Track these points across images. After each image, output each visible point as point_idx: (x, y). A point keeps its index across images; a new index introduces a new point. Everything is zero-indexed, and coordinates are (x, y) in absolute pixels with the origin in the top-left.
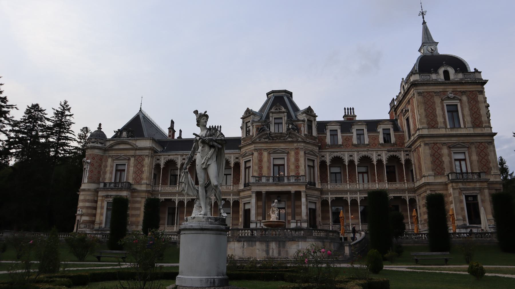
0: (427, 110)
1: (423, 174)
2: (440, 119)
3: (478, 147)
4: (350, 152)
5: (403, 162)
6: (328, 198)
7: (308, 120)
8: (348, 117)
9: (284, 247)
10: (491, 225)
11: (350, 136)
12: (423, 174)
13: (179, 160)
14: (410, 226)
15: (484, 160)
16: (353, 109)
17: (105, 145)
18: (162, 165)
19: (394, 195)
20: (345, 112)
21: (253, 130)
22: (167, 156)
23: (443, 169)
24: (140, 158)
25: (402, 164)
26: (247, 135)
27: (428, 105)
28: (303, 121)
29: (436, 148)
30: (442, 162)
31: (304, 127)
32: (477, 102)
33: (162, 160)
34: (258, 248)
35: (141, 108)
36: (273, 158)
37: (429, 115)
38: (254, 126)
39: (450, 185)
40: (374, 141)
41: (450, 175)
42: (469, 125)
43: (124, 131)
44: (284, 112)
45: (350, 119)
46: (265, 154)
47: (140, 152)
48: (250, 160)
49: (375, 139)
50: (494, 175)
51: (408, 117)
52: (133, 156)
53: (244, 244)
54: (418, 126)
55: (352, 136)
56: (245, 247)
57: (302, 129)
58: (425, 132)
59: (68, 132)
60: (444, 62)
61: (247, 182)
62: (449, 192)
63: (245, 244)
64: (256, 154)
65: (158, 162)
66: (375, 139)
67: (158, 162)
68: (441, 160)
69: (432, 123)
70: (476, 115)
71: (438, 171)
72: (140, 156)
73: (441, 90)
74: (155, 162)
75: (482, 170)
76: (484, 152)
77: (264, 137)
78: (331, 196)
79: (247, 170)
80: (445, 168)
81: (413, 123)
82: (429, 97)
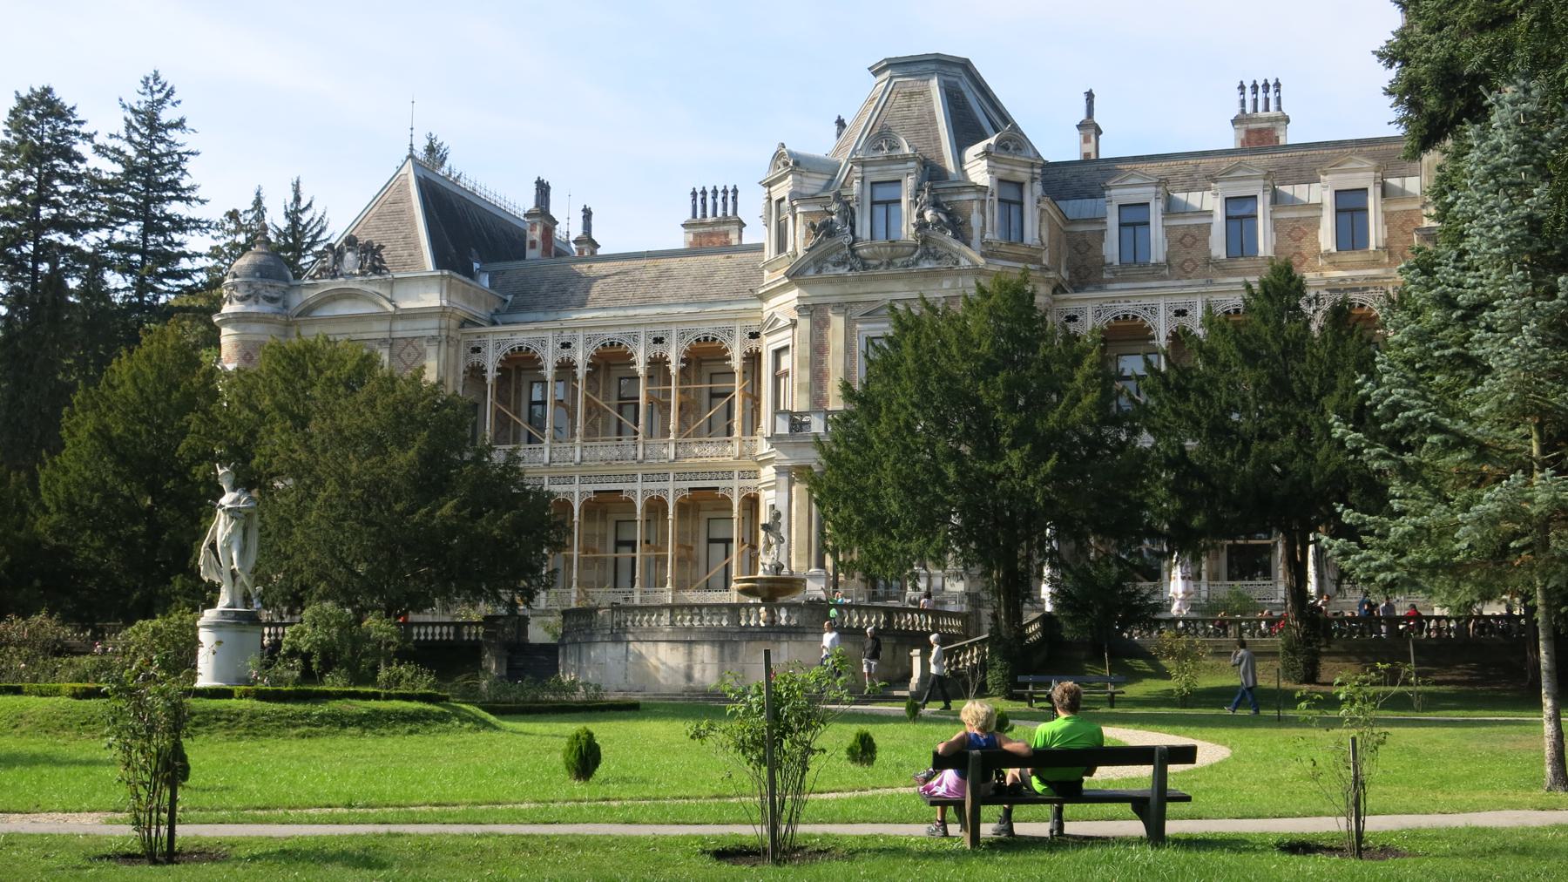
4: (1176, 300)
7: (1001, 181)
8: (1253, 126)
11: (1198, 226)
13: (550, 348)
16: (1277, 85)
17: (286, 307)
18: (490, 371)
20: (1243, 102)
22: (507, 336)
24: (410, 349)
31: (983, 213)
33: (490, 351)
35: (412, 149)
40: (1297, 244)
43: (349, 250)
45: (1260, 131)
46: (837, 323)
47: (409, 325)
52: (385, 340)
55: (1209, 225)
57: (975, 219)
59: (179, 198)
64: (805, 324)
65: (476, 358)
67: (476, 358)
72: (409, 341)
74: (466, 358)
77: (833, 258)
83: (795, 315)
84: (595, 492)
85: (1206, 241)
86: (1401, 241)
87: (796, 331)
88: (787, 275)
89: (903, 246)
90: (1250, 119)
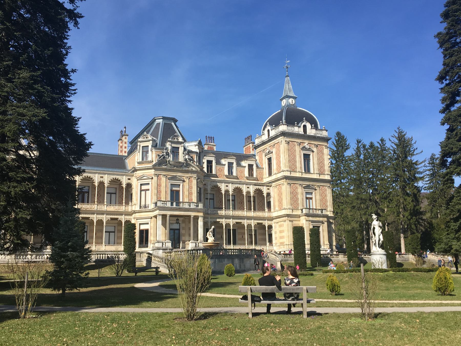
1: (284, 207)
2: (298, 165)
5: (265, 195)
6: (208, 221)
9: (243, 263)
12: (284, 207)
14: (268, 247)
15: (324, 200)
23: (298, 204)
26: (143, 159)
28: (196, 153)
30: (297, 199)
32: (323, 154)
38: (154, 152)
39: (304, 217)
41: (304, 210)
44: (181, 143)
45: (211, 147)
48: (149, 183)
53: (215, 261)
54: (283, 168)
56: (216, 262)
58: (288, 174)
60: (304, 118)
61: (143, 203)
62: (302, 223)
63: (216, 260)
64: (155, 178)
73: (301, 141)
79: (143, 193)
81: (277, 164)
84: (110, 218)
87: (153, 180)
88: (153, 166)
90: (209, 145)
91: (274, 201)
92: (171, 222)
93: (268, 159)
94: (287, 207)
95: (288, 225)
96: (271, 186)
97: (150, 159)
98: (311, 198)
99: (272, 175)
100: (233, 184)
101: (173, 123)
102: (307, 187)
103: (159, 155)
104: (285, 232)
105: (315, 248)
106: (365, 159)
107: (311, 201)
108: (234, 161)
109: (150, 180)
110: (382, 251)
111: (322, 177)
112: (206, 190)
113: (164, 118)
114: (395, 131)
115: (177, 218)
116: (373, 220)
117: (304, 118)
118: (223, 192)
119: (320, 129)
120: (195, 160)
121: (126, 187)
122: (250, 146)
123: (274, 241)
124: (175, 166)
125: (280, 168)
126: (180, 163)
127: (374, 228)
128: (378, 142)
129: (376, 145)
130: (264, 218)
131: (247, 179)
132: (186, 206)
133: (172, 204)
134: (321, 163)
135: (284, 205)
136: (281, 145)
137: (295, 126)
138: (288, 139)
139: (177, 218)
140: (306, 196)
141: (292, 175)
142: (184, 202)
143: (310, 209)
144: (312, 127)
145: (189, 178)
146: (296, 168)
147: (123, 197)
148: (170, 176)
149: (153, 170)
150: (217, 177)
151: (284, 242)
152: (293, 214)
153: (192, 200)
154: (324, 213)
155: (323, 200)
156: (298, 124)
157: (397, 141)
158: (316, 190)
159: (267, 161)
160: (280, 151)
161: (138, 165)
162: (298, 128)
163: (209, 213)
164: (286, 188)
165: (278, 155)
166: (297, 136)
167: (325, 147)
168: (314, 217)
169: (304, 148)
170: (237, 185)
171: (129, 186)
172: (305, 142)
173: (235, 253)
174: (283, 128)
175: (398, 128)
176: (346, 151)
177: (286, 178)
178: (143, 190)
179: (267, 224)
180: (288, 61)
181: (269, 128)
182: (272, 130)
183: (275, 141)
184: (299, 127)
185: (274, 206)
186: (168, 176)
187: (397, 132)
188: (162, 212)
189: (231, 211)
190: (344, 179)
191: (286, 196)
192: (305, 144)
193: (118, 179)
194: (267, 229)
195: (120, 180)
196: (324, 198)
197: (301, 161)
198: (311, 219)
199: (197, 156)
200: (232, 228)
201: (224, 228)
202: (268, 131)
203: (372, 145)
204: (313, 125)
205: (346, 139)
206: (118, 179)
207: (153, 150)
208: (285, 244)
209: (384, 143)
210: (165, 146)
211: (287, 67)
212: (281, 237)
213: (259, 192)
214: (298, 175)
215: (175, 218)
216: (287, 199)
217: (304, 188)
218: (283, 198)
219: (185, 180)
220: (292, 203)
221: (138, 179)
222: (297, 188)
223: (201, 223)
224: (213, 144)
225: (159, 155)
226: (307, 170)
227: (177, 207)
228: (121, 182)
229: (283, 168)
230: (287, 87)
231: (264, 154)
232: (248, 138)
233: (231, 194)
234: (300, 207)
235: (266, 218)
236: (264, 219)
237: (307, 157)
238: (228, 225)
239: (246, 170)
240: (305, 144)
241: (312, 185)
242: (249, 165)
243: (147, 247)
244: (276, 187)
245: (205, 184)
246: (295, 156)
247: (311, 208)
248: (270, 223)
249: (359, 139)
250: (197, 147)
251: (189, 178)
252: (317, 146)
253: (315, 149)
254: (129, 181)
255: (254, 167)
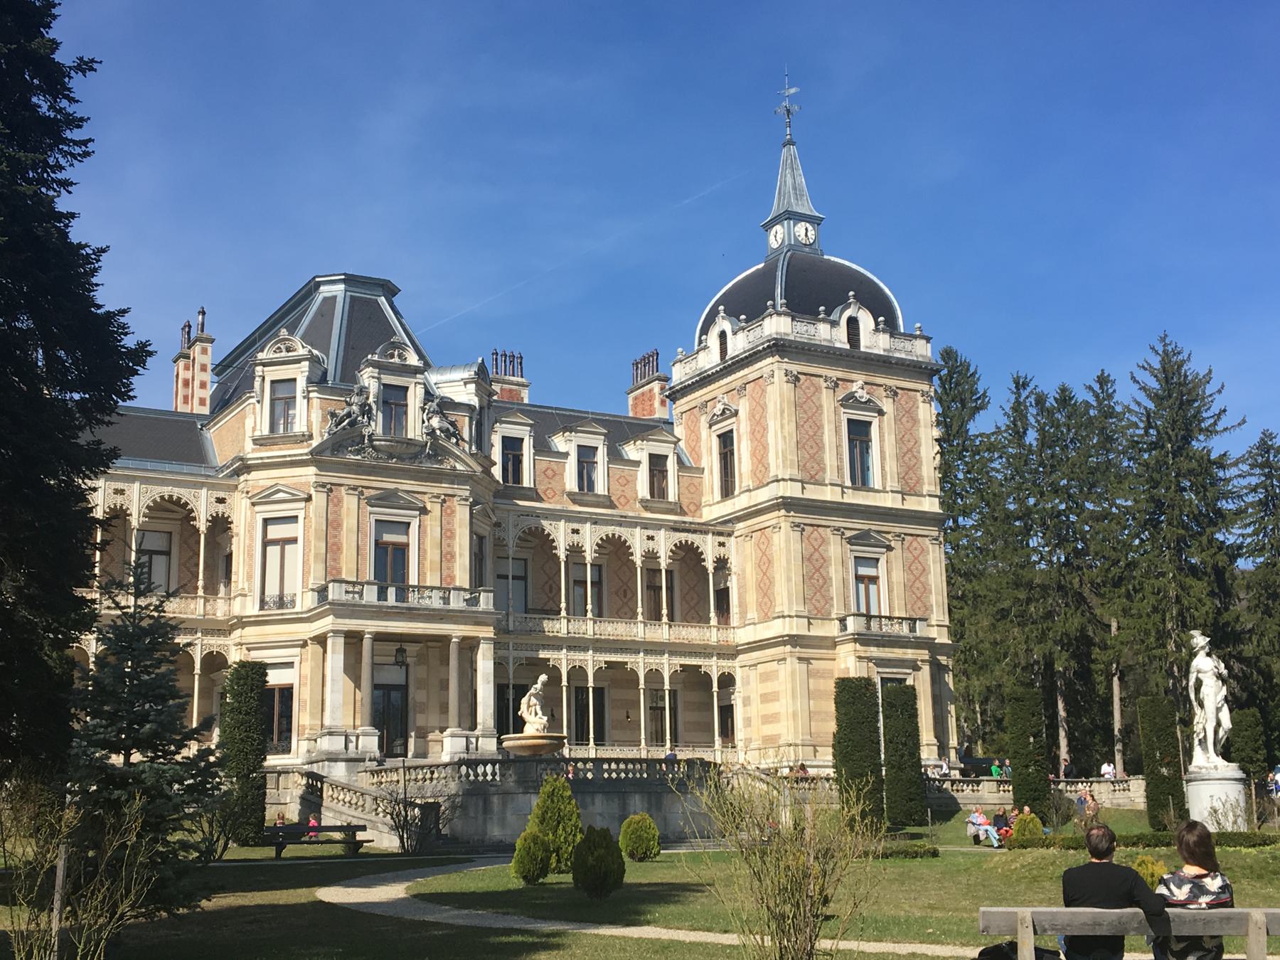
0: (803, 426)
1: (777, 610)
2: (829, 459)
3: (908, 548)
5: (710, 565)
10: (932, 757)
12: (777, 610)
15: (918, 584)
19: (682, 662)
21: (308, 416)
23: (828, 600)
25: (707, 570)
26: (273, 428)
27: (805, 412)
28: (469, 407)
29: (816, 540)
30: (826, 581)
32: (915, 421)
34: (600, 811)
36: (376, 520)
37: (807, 440)
38: (316, 402)
39: (851, 646)
40: (623, 488)
42: (892, 484)
44: (414, 371)
45: (511, 390)
48: (297, 517)
49: (625, 482)
50: (938, 626)
51: (731, 431)
54: (776, 469)
58: (793, 490)
60: (851, 293)
61: (272, 590)
62: (843, 666)
64: (319, 499)
66: (625, 482)
68: (825, 574)
69: (813, 468)
70: (910, 459)
71: (818, 605)
73: (840, 374)
75: (913, 610)
76: (920, 563)
78: (515, 653)
79: (273, 551)
80: (832, 599)
81: (753, 454)
82: (809, 389)
83: (312, 492)
85: (562, 475)
86: (688, 498)
87: (312, 506)
88: (311, 453)
89: (416, 445)
91: (742, 588)
92: (378, 659)
93: (719, 436)
94: (790, 609)
95: (793, 672)
96: (730, 535)
97: (299, 427)
98: (874, 580)
99: (736, 492)
100: (595, 523)
101: (382, 300)
102: (861, 538)
103: (333, 415)
104: (783, 701)
105: (902, 756)
106: (1045, 442)
107: (873, 588)
108: (599, 442)
109: (302, 504)
110: (1232, 770)
111: (912, 504)
112: (499, 543)
113: (350, 280)
114: (1153, 348)
115: (398, 645)
116: (1193, 654)
117: (851, 293)
118: (562, 554)
119: (904, 335)
120: (466, 436)
121: (208, 529)
122: (651, 390)
123: (740, 733)
124: (391, 456)
125: (767, 468)
126: (410, 443)
127: (1199, 683)
128: (1090, 388)
129: (1082, 395)
130: (706, 647)
131: (646, 509)
132: (435, 602)
133: (382, 595)
134: (909, 455)
135: (778, 601)
136: (769, 388)
137: (820, 321)
138: (795, 368)
139: (398, 645)
140: (856, 571)
141: (808, 495)
142: (427, 588)
143: (869, 617)
144: (877, 324)
145: (444, 501)
146: (823, 470)
147: (198, 565)
148: (373, 492)
149: (312, 470)
150: (540, 499)
151: (779, 736)
152: (812, 633)
153: (453, 578)
154: (918, 634)
155: (916, 587)
156: (828, 313)
157: (1153, 384)
158: (890, 548)
159: (715, 443)
160: (764, 408)
161: (253, 450)
162: (828, 326)
163: (511, 628)
164: (788, 541)
165: (758, 423)
166: (827, 355)
167: (922, 399)
168: (884, 646)
169: (849, 401)
170: (610, 530)
171: (221, 525)
172: (854, 376)
173: (630, 775)
174: (776, 325)
175: (1163, 339)
176: (977, 416)
177: (788, 504)
178: (274, 542)
179: (714, 668)
180: (793, 91)
181: (723, 324)
182: (735, 333)
183: (746, 371)
184: (834, 324)
185: (742, 604)
186: (367, 493)
187: (1157, 353)
188: (347, 621)
189: (590, 623)
190: (966, 514)
191: (789, 570)
192: (855, 387)
193: (179, 499)
194: (715, 688)
195: (187, 504)
196: (917, 579)
197: (839, 446)
198: (875, 655)
199: (471, 419)
200: (591, 684)
201: (564, 683)
202: (723, 335)
203: (1065, 398)
204: (881, 319)
205: (973, 375)
206: (179, 499)
207: (312, 395)
208: (781, 742)
209: (1110, 391)
210: (355, 380)
211: (788, 111)
212: (768, 719)
213: (688, 556)
214: (829, 494)
215: (395, 646)
216: (789, 579)
217: (851, 541)
218: (777, 577)
219: (429, 507)
220: (809, 594)
221: (254, 500)
222: (824, 541)
223: (485, 664)
224: (520, 379)
225: (333, 415)
226: (860, 477)
227: (399, 604)
228: (192, 511)
229: (776, 469)
230: (789, 180)
231: (704, 420)
232: (646, 360)
233: (589, 559)
234: (836, 611)
235: (714, 647)
236: (705, 651)
237: (859, 432)
238: (577, 673)
239: (643, 474)
240: (855, 387)
241: (879, 532)
242: (652, 457)
243: (287, 750)
244: (750, 535)
245: (498, 525)
246: (820, 427)
247: (872, 614)
248: (726, 665)
249: (1022, 374)
250: (472, 387)
251: (444, 500)
252: (896, 394)
253: (887, 405)
254: (221, 508)
255: (671, 465)
